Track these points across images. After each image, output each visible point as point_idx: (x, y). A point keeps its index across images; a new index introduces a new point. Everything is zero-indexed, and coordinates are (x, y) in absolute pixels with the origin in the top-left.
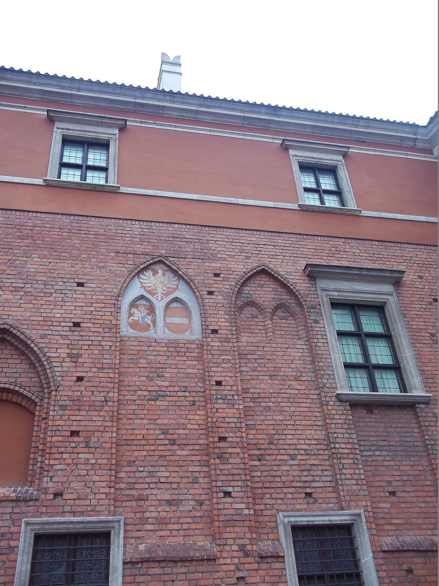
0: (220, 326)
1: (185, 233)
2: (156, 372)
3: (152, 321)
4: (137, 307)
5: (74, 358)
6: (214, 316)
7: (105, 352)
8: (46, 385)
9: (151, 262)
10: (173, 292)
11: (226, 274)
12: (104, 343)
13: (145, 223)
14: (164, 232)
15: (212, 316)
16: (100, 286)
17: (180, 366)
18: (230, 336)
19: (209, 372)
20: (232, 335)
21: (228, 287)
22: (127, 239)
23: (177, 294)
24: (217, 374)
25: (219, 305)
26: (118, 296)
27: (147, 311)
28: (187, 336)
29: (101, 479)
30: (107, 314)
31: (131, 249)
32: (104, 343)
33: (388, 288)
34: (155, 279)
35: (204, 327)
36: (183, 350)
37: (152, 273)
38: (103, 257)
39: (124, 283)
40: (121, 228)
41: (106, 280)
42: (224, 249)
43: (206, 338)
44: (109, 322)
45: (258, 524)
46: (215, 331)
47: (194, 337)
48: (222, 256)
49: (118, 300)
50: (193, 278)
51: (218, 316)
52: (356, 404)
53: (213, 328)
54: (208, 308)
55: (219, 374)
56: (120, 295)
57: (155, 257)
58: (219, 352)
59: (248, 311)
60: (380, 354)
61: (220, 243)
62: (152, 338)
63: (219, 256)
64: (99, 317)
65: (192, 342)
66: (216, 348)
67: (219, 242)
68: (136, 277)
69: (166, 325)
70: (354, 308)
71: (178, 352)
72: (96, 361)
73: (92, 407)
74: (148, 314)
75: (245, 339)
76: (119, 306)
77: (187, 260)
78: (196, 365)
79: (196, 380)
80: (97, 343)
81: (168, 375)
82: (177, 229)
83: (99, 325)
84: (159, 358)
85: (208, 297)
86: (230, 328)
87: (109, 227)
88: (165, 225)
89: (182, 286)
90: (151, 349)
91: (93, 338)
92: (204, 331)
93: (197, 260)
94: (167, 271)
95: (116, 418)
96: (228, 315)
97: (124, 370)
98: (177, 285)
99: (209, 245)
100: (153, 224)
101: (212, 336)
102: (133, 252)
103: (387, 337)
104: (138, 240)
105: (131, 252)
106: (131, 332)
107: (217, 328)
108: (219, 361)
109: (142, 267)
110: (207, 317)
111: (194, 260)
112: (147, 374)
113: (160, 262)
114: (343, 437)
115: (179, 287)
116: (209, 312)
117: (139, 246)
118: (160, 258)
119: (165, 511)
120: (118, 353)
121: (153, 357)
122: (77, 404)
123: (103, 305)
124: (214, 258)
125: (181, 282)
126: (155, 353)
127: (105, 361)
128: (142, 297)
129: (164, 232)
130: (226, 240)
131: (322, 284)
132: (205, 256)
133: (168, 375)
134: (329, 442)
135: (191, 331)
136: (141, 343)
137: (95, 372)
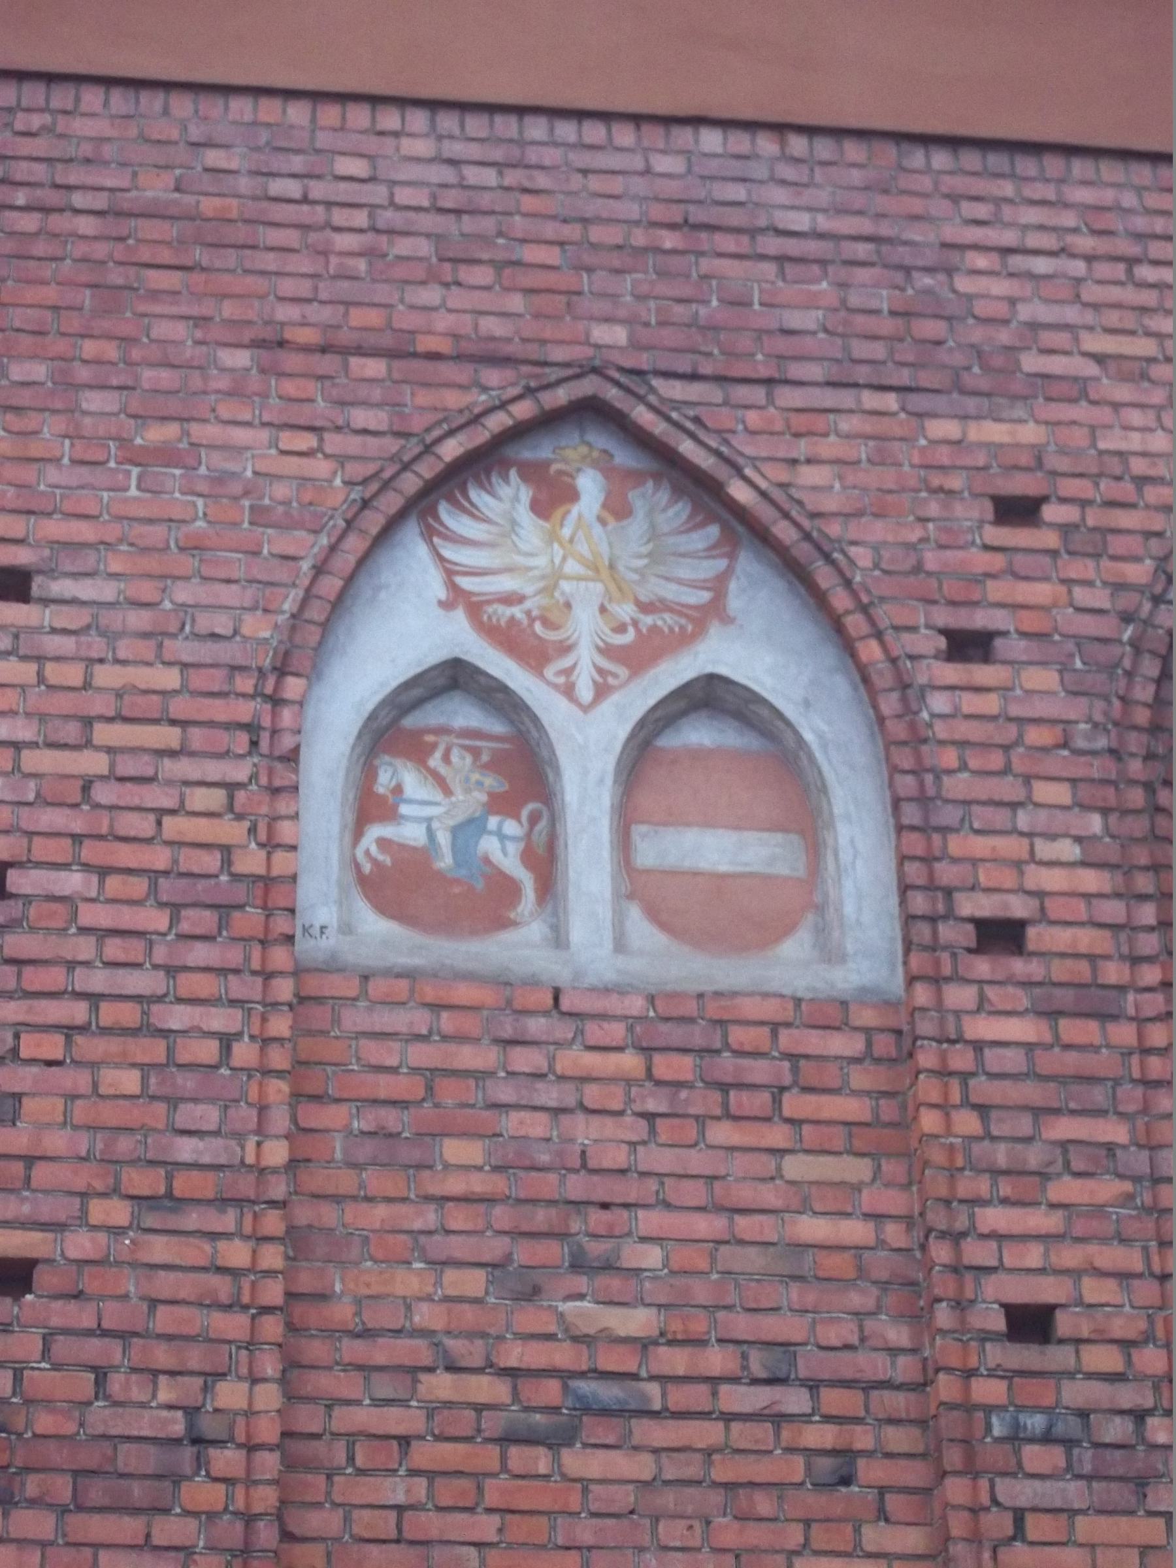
0: (1040, 895)
1: (780, 195)
2: (562, 1230)
3: (529, 857)
4: (416, 749)
6: (1000, 818)
7: (187, 1082)
9: (524, 410)
10: (683, 640)
11: (1084, 503)
12: (177, 1017)
13: (476, 124)
14: (616, 185)
15: (981, 816)
16: (146, 590)
17: (745, 1194)
18: (1113, 973)
19: (956, 1238)
20: (1136, 960)
21: (1099, 598)
22: (345, 242)
23: (721, 654)
25: (1036, 736)
26: (282, 671)
27: (491, 781)
28: (791, 967)
30: (200, 799)
31: (373, 317)
32: (177, 1017)
34: (552, 537)
35: (919, 903)
36: (759, 1071)
37: (525, 494)
38: (166, 378)
39: (319, 570)
40: (297, 163)
41: (193, 547)
42: (1071, 314)
43: (937, 981)
44: (210, 862)
46: (999, 935)
47: (848, 978)
48: (1056, 365)
49: (276, 701)
50: (834, 529)
51: (1023, 820)
53: (984, 906)
54: (950, 757)
55: (1033, 1256)
56: (297, 658)
57: (554, 374)
58: (1031, 1092)
61: (1041, 265)
62: (532, 982)
63: (1031, 362)
64: (143, 825)
65: (831, 1014)
66: (1013, 1060)
68: (411, 532)
69: (636, 884)
71: (724, 1088)
72: (125, 1145)
74: (502, 804)
76: (287, 742)
77: (789, 397)
78: (857, 1188)
79: (856, 1299)
80: (129, 1014)
81: (652, 1257)
82: (713, 166)
83: (138, 886)
84: (584, 1131)
85: (951, 673)
86: (1114, 911)
87: (213, 158)
88: (625, 135)
89: (757, 594)
90: (524, 1060)
91: (97, 980)
92: (923, 931)
93: (871, 400)
94: (636, 477)
96: (1105, 811)
97: (329, 1215)
98: (719, 585)
99: (963, 284)
100: (537, 128)
101: (982, 967)
102: (387, 340)
104: (424, 247)
105: (372, 340)
106: (376, 936)
107: (1019, 908)
108: (1034, 1157)
109: (451, 449)
110: (944, 830)
111: (846, 399)
112: (494, 1248)
113: (591, 410)
115: (735, 603)
116: (958, 785)
117: (431, 295)
118: (588, 387)
120: (278, 1089)
121: (537, 1125)
123: (170, 736)
125: (749, 564)
126: (549, 1094)
127: (186, 1149)
128: (455, 677)
129: (616, 185)
130: (1086, 243)
132: (931, 361)
133: (652, 1257)
135: (821, 931)
136: (447, 1021)
137: (117, 1231)
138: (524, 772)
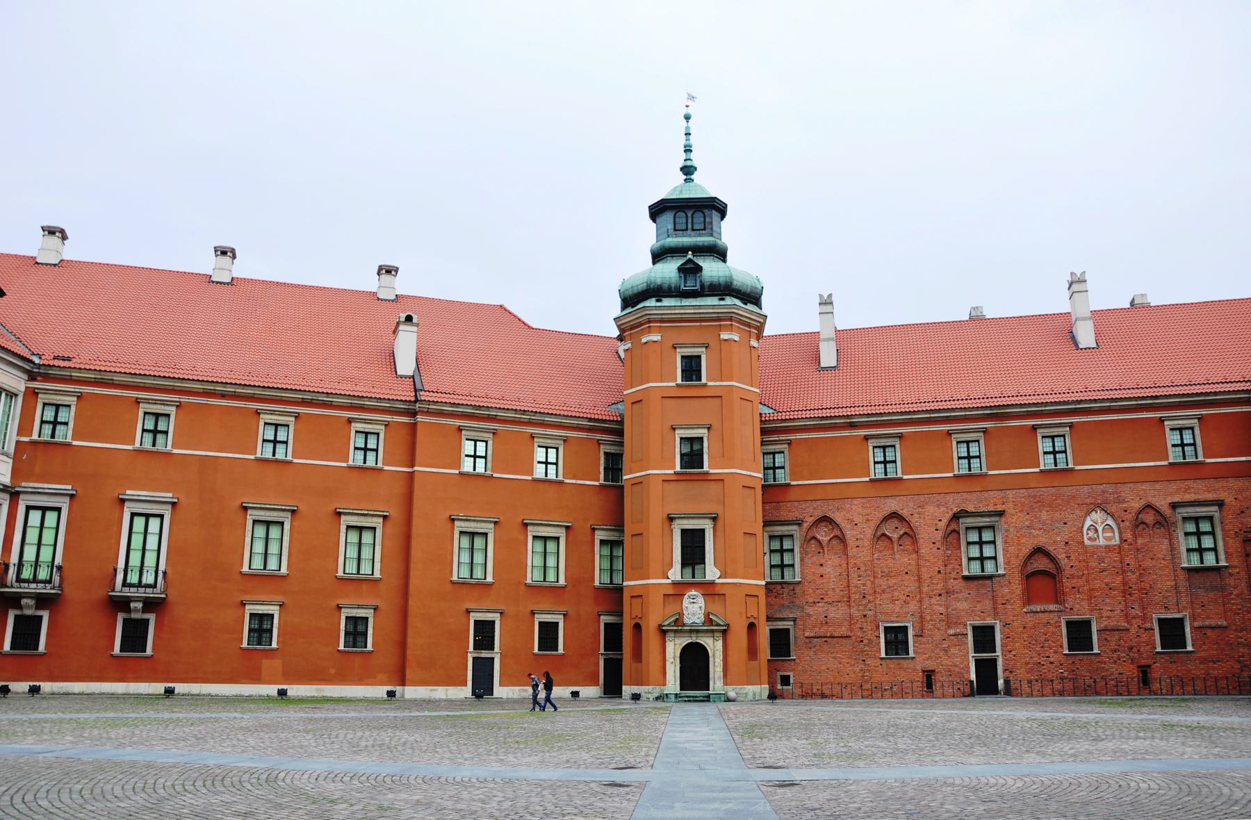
2: (1101, 560)
5: (1068, 557)
24: (1127, 560)
28: (1113, 543)
29: (1085, 604)
33: (1216, 508)
45: (1145, 618)
52: (1190, 570)
59: (1141, 526)
60: (1207, 542)
67: (1126, 491)
70: (1197, 520)
73: (1078, 577)
75: (1140, 541)
95: (1087, 581)
103: (1212, 533)
114: (1183, 584)
119: (1109, 614)
124: (1124, 502)
131: (1179, 510)
132: (1120, 501)
134: (1176, 587)
138: (1096, 531)
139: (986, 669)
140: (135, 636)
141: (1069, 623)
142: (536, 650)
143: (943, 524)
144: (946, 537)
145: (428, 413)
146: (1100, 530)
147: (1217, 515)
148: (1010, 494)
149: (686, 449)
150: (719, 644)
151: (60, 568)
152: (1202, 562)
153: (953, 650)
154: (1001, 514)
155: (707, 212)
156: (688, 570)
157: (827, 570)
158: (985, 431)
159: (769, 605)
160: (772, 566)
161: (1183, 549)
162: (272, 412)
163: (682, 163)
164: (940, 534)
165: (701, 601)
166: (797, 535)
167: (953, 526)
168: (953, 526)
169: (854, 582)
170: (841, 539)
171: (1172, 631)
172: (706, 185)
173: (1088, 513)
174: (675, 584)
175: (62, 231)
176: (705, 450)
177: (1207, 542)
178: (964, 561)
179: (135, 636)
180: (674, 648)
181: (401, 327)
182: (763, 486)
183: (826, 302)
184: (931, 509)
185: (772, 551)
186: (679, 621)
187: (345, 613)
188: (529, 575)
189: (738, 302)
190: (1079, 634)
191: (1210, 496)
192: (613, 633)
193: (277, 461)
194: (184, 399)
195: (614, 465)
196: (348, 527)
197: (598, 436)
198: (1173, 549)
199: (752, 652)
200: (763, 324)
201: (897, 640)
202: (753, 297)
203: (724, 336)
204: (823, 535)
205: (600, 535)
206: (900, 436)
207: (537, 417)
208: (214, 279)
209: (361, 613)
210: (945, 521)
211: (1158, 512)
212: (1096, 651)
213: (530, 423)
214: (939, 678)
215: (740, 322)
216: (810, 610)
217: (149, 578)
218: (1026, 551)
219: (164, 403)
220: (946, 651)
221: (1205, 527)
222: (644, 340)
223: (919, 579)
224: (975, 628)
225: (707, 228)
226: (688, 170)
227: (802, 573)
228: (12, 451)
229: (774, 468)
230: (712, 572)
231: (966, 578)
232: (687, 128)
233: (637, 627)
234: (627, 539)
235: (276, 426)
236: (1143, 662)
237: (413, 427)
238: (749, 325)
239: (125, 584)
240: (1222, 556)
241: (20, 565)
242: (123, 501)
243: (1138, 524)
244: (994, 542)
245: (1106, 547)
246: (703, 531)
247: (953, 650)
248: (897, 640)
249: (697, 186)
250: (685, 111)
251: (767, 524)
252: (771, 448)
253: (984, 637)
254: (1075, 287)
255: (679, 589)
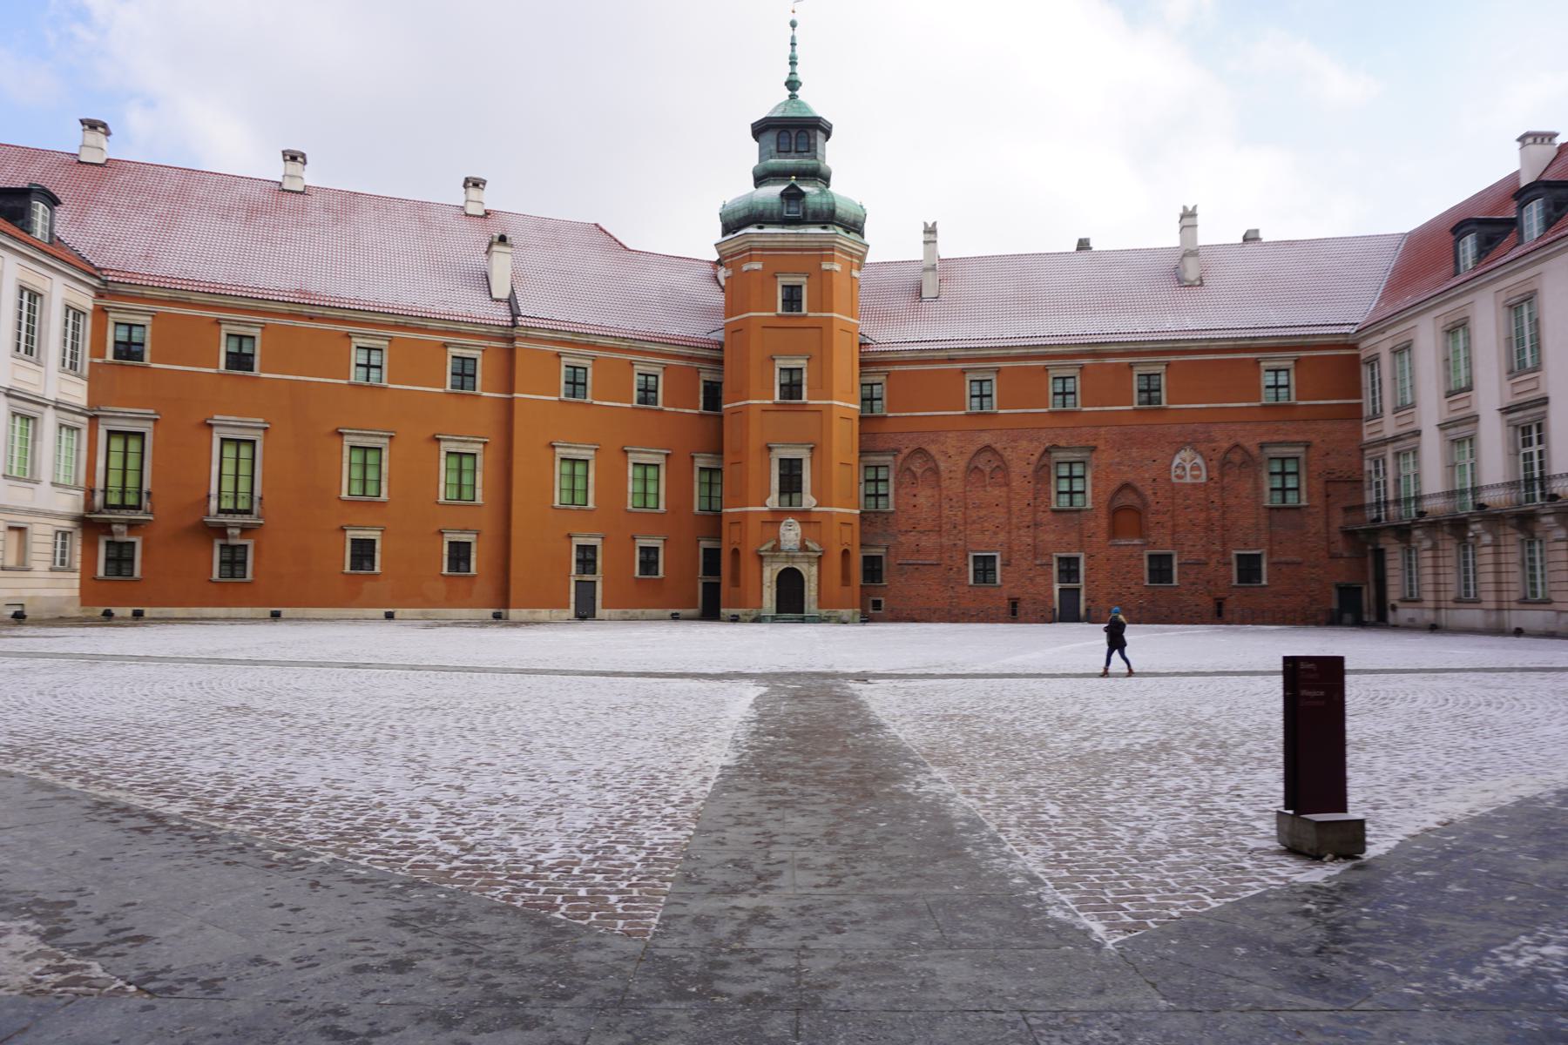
2: (1187, 497)
8: (1145, 505)
24: (1212, 498)
29: (1168, 539)
45: (1225, 553)
52: (1271, 509)
60: (1291, 482)
122: (1157, 512)
132: (1210, 440)
139: (1069, 596)
140: (234, 560)
141: (1151, 557)
142: (637, 574)
143: (1034, 459)
144: (1036, 471)
145: (527, 338)
146: (1188, 466)
147: (1303, 456)
148: (1103, 430)
149: (786, 380)
150: (814, 569)
151: (149, 494)
152: (1284, 501)
153: (1038, 579)
154: (1093, 449)
155: (810, 132)
156: (786, 499)
157: (921, 500)
158: (1082, 368)
159: (862, 533)
160: (867, 496)
161: (1267, 489)
162: (364, 336)
163: (785, 78)
164: (1032, 468)
165: (797, 528)
166: (892, 466)
167: (1045, 461)
168: (1045, 461)
169: (946, 512)
170: (936, 471)
171: (1249, 568)
172: (814, 101)
173: (1177, 451)
174: (773, 512)
175: (104, 125)
176: (804, 381)
177: (1291, 482)
178: (1054, 494)
179: (234, 560)
180: (770, 574)
181: (495, 248)
182: (861, 418)
183: (931, 231)
184: (1024, 444)
185: (867, 481)
186: (776, 548)
187: (448, 537)
188: (630, 501)
189: (840, 231)
190: (1160, 568)
191: (1298, 438)
192: (712, 560)
193: (371, 387)
194: (269, 320)
195: (713, 396)
196: (448, 453)
197: (697, 365)
198: (1258, 488)
199: (846, 578)
200: (865, 254)
201: (985, 567)
202: (855, 226)
203: (826, 266)
204: (917, 466)
205: (700, 462)
206: (998, 371)
207: (637, 344)
208: (286, 187)
209: (464, 538)
210: (1037, 455)
211: (1246, 452)
212: (1175, 583)
213: (629, 351)
214: (1023, 607)
215: (842, 251)
216: (902, 539)
217: (242, 505)
218: (1114, 487)
219: (247, 324)
220: (1031, 580)
221: (1290, 467)
222: (745, 268)
223: (1009, 511)
224: (1060, 559)
225: (811, 150)
226: (792, 85)
227: (896, 502)
228: (86, 372)
229: (872, 399)
230: (808, 501)
231: (1054, 511)
232: (793, 38)
233: (736, 552)
234: (726, 469)
235: (369, 349)
236: (1220, 595)
237: (511, 353)
238: (851, 255)
239: (220, 511)
240: (1304, 497)
241: (106, 491)
242: (211, 426)
243: (1225, 464)
244: (1083, 477)
245: (1194, 485)
246: (801, 460)
247: (1038, 579)
248: (985, 567)
249: (800, 103)
250: (791, 17)
251: (863, 452)
252: (870, 380)
253: (1069, 569)
254: (1187, 221)
255: (777, 517)
